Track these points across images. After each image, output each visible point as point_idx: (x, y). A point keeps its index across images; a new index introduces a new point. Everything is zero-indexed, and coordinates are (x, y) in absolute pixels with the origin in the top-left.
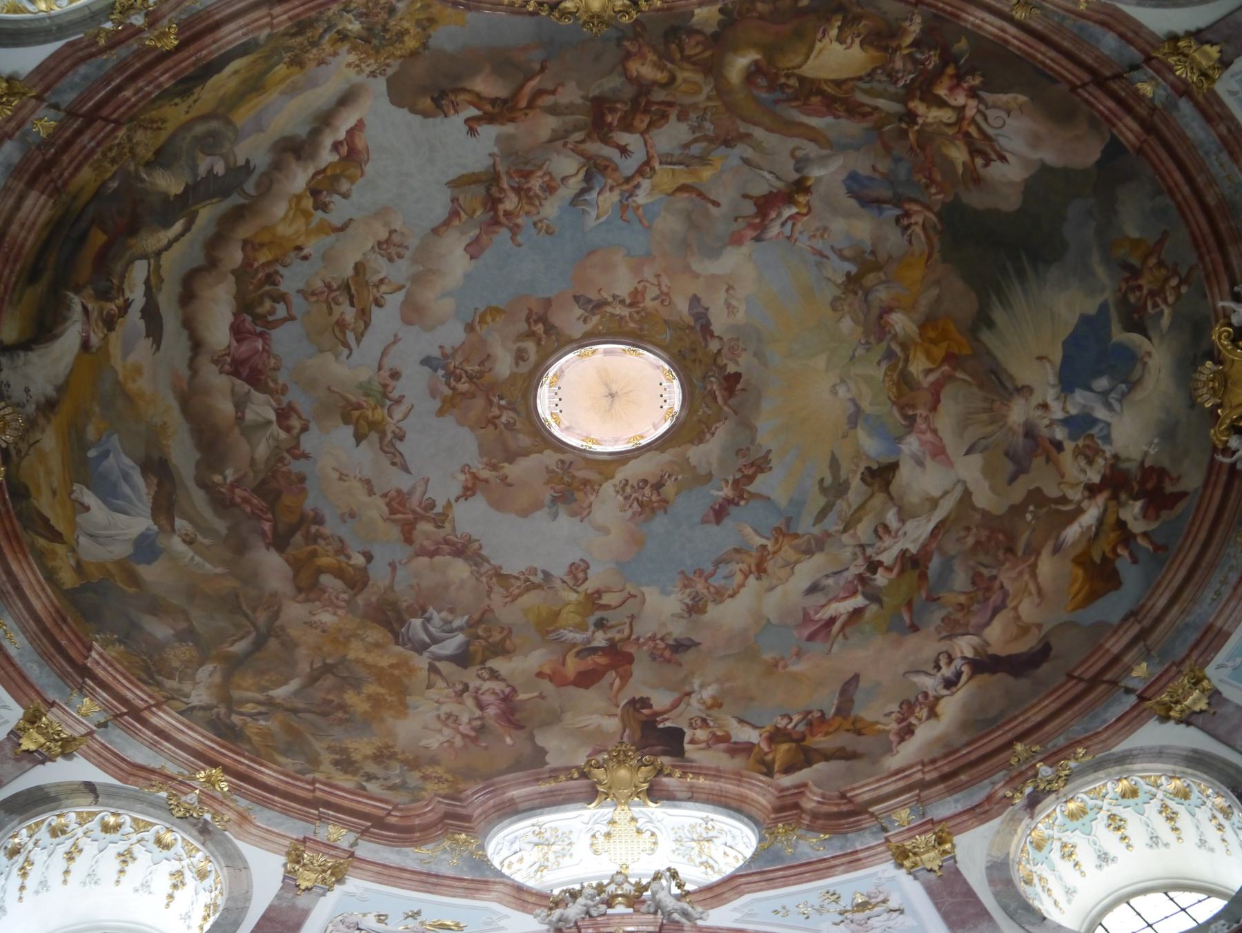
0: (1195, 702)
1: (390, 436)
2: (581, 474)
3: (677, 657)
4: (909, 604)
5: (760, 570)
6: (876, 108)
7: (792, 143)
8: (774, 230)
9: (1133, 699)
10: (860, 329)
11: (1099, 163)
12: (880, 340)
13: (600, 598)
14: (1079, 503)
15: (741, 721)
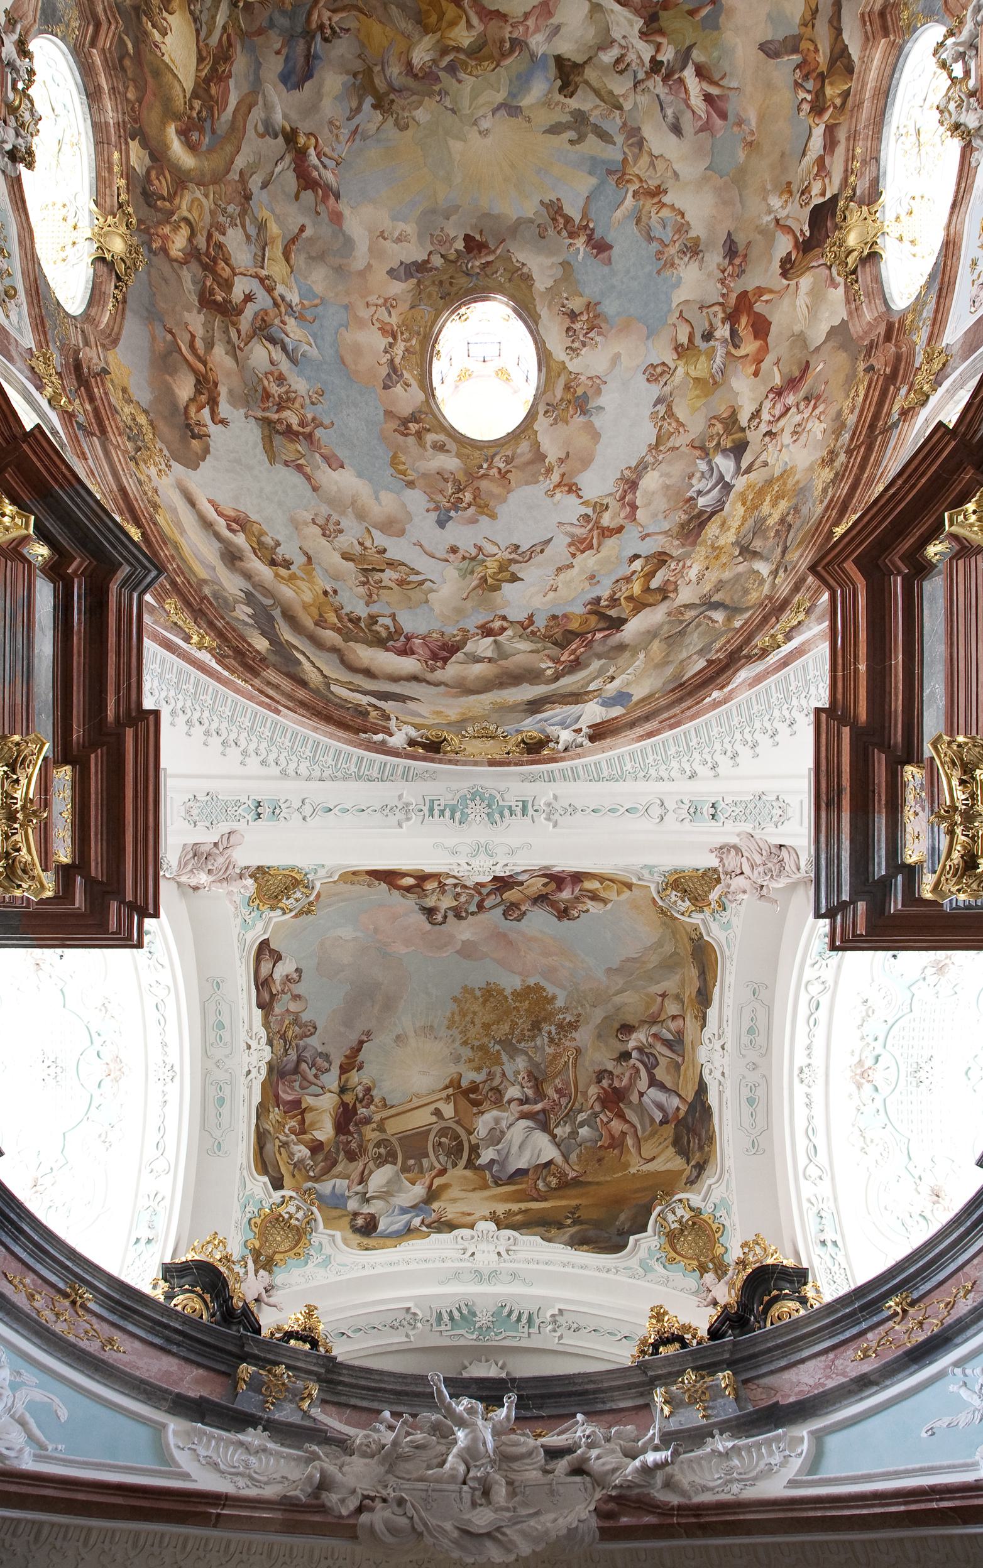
1: (513, 556)
2: (559, 392)
3: (741, 248)
6: (224, 28)
8: (329, 177)
12: (438, 79)
13: (682, 345)
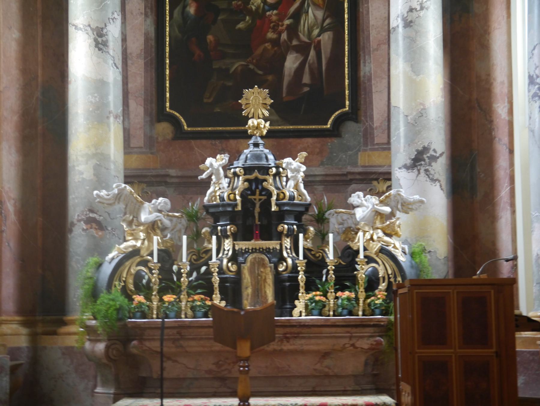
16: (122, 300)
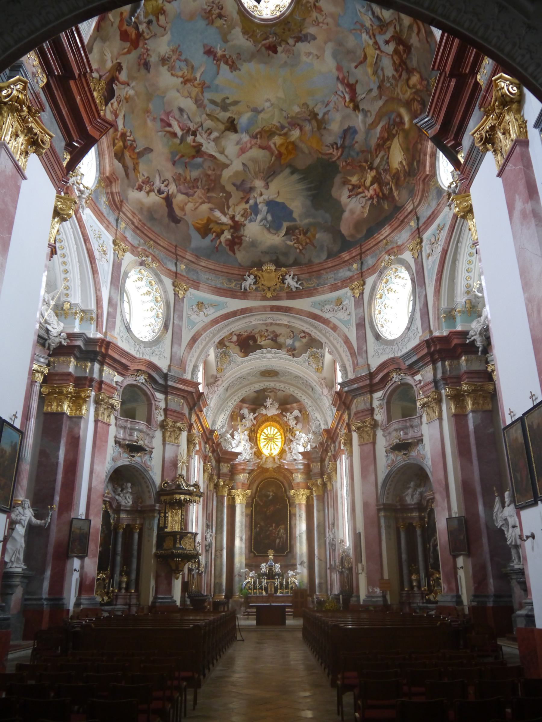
0: (181, 294)
3: (142, 66)
4: (182, 156)
5: (185, 82)
6: (377, 156)
7: (374, 114)
8: (341, 88)
9: (173, 269)
10: (294, 115)
11: (340, 231)
12: (289, 123)
13: (162, 14)
14: (228, 214)
15: (124, 116)
16: (247, 591)
